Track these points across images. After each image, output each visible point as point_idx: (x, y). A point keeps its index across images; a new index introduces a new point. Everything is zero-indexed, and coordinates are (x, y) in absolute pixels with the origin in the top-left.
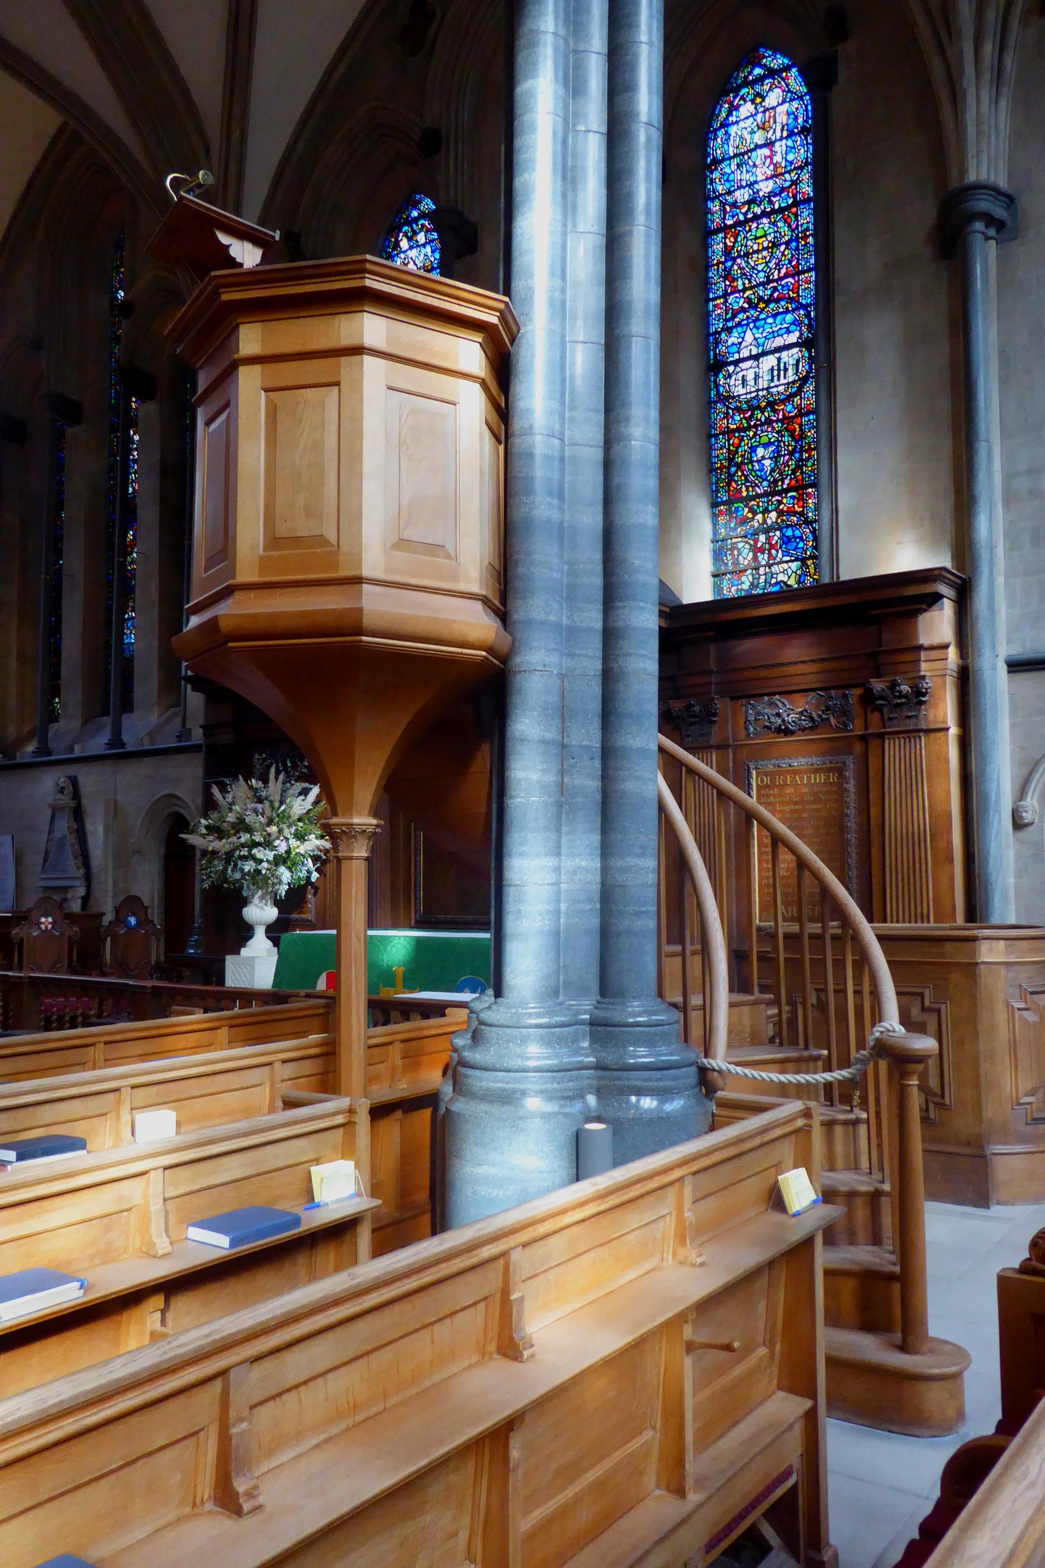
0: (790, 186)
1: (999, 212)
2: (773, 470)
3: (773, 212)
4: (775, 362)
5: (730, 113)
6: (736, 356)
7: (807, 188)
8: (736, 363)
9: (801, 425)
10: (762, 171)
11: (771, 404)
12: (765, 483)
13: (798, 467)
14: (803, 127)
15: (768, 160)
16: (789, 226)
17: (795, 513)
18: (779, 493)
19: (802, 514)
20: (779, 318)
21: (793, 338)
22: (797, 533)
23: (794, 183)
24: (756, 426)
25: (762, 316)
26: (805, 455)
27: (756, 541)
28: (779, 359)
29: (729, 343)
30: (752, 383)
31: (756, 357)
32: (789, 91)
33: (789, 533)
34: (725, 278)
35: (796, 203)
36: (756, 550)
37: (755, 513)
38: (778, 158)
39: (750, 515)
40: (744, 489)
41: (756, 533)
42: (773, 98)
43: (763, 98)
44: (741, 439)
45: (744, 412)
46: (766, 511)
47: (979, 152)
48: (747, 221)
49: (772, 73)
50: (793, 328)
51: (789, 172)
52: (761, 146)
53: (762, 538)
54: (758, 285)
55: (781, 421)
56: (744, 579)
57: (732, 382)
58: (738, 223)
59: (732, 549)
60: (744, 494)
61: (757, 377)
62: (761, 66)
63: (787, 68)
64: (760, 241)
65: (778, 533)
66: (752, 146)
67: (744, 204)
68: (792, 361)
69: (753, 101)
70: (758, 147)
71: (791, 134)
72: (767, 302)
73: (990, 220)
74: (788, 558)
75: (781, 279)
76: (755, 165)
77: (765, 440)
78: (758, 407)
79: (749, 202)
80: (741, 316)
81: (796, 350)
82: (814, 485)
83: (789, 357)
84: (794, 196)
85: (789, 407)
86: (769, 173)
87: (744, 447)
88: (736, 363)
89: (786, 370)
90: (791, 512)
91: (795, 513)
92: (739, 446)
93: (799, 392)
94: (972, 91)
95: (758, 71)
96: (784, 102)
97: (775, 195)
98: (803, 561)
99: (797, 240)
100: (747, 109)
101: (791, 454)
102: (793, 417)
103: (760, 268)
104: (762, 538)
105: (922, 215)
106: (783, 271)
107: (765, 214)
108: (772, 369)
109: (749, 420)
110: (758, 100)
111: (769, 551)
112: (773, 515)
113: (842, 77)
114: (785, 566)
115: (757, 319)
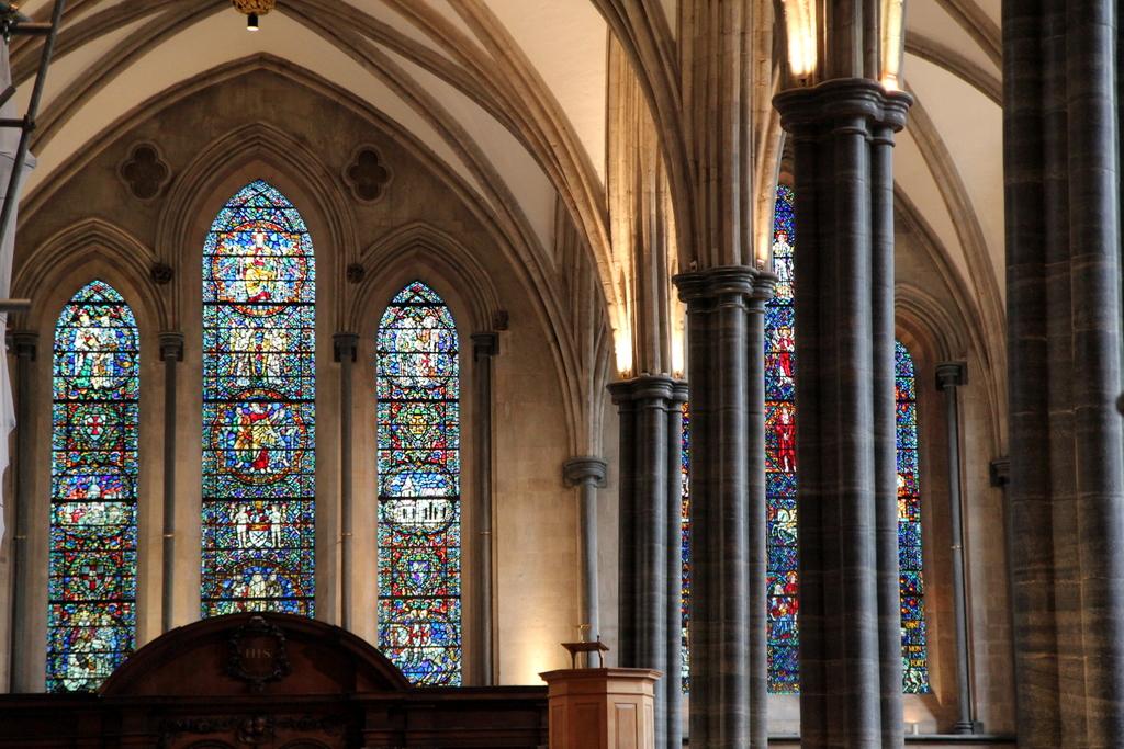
0: (440, 387)
1: (601, 474)
2: (425, 581)
3: (428, 400)
4: (428, 506)
5: (396, 320)
6: (399, 495)
7: (453, 391)
8: (399, 499)
9: (446, 553)
10: (419, 370)
11: (425, 535)
12: (420, 589)
13: (445, 581)
14: (450, 350)
15: (424, 365)
16: (439, 414)
17: (441, 614)
18: (430, 598)
19: (446, 615)
20: (431, 476)
21: (441, 492)
22: (442, 628)
23: (443, 385)
24: (413, 547)
25: (420, 471)
26: (449, 575)
27: (412, 628)
28: (431, 504)
29: (393, 483)
30: (411, 516)
31: (415, 499)
32: (440, 321)
33: (437, 627)
34: (392, 437)
35: (444, 400)
36: (412, 636)
37: (411, 609)
38: (432, 364)
39: (407, 609)
40: (403, 590)
41: (412, 623)
42: (429, 322)
43: (423, 319)
44: (402, 555)
45: (404, 535)
46: (419, 608)
47: (594, 440)
48: (408, 401)
49: (427, 304)
50: (441, 485)
51: (440, 377)
52: (420, 352)
53: (417, 627)
54: (416, 449)
55: (432, 548)
56: (402, 654)
57: (395, 511)
58: (400, 400)
59: (394, 632)
60: (404, 594)
61: (414, 512)
62: (420, 296)
63: (440, 305)
64: (418, 417)
65: (428, 626)
66: (413, 350)
67: (406, 388)
68: (440, 508)
69: (413, 318)
70: (417, 352)
71: (440, 353)
72: (424, 464)
73: (598, 478)
74: (434, 645)
75: (435, 449)
76: (415, 364)
77: (419, 558)
78: (415, 535)
79: (412, 388)
80: (403, 467)
81: (444, 501)
82: (455, 597)
83: (439, 504)
84: (444, 394)
85: (438, 540)
86: (426, 372)
87: (404, 560)
88: (399, 499)
89: (436, 513)
90: (438, 612)
91: (441, 614)
92: (400, 558)
93: (445, 530)
94: (592, 404)
95: (417, 298)
96: (436, 328)
97: (430, 389)
98: (447, 648)
99: (445, 426)
100: (408, 322)
101: (439, 572)
102: (440, 547)
103: (418, 437)
104: (417, 627)
105: (552, 459)
106: (434, 443)
107: (421, 400)
108: (426, 510)
109: (408, 541)
110: (418, 319)
111: (422, 637)
112: (425, 612)
113: (502, 350)
114: (433, 649)
115: (414, 473)
